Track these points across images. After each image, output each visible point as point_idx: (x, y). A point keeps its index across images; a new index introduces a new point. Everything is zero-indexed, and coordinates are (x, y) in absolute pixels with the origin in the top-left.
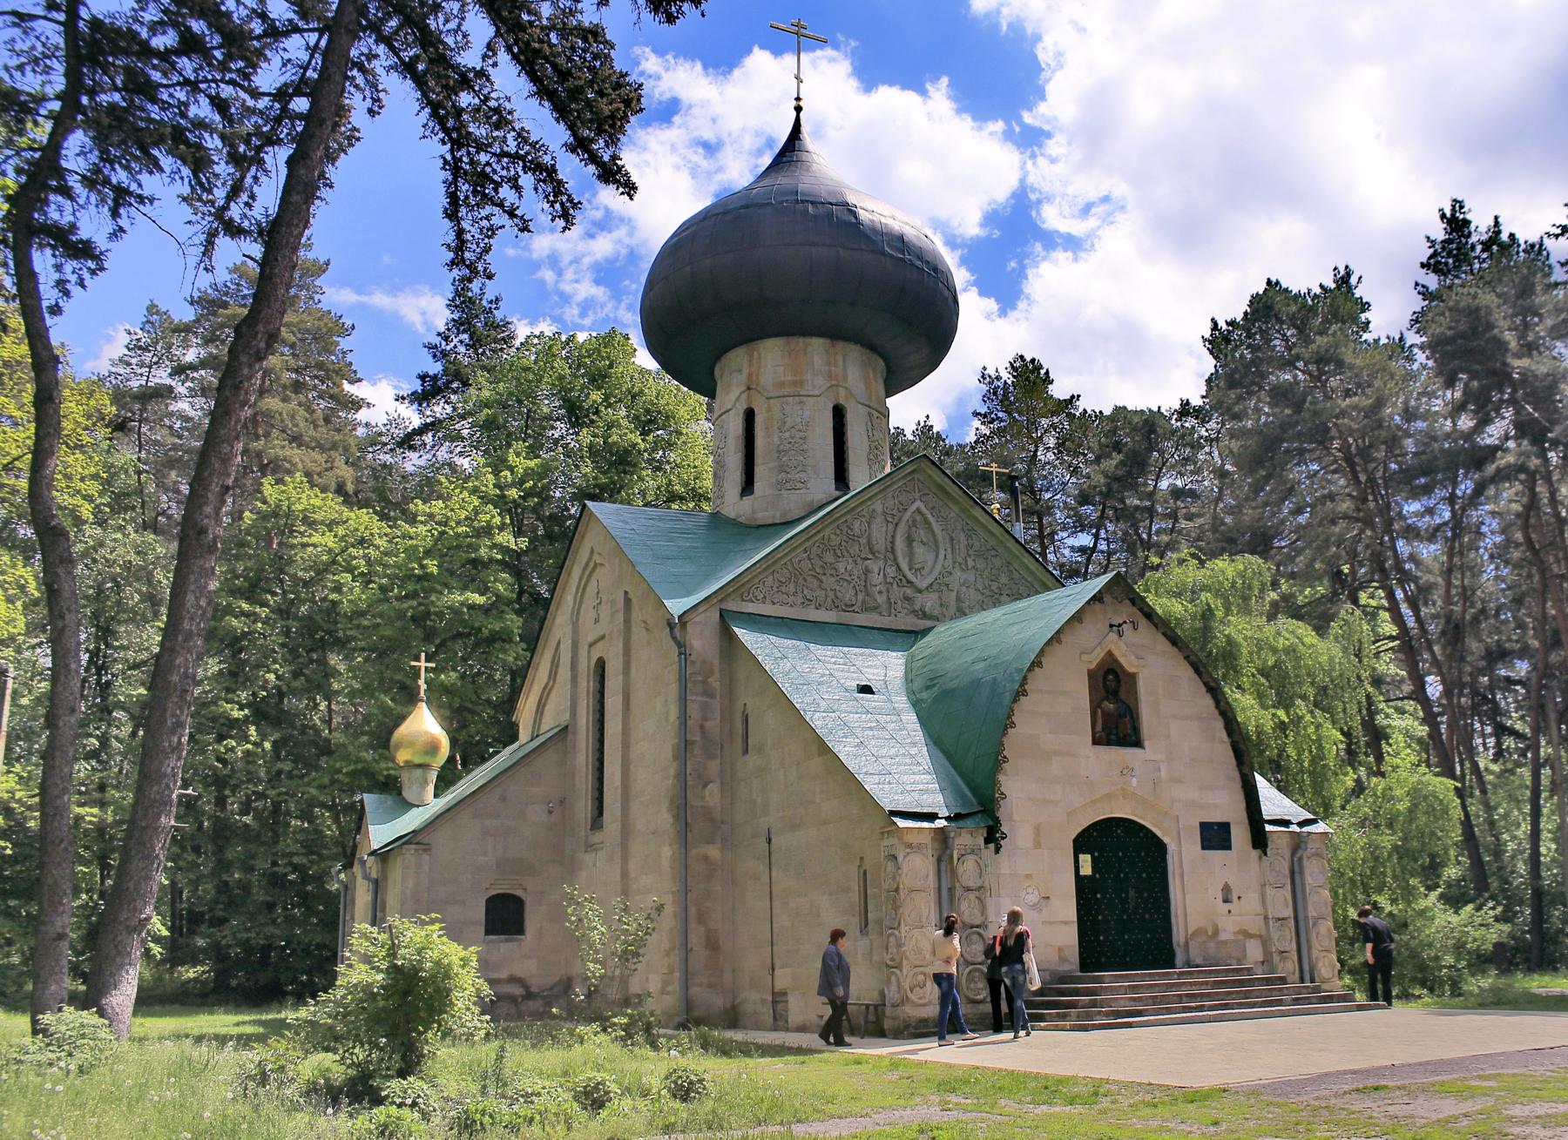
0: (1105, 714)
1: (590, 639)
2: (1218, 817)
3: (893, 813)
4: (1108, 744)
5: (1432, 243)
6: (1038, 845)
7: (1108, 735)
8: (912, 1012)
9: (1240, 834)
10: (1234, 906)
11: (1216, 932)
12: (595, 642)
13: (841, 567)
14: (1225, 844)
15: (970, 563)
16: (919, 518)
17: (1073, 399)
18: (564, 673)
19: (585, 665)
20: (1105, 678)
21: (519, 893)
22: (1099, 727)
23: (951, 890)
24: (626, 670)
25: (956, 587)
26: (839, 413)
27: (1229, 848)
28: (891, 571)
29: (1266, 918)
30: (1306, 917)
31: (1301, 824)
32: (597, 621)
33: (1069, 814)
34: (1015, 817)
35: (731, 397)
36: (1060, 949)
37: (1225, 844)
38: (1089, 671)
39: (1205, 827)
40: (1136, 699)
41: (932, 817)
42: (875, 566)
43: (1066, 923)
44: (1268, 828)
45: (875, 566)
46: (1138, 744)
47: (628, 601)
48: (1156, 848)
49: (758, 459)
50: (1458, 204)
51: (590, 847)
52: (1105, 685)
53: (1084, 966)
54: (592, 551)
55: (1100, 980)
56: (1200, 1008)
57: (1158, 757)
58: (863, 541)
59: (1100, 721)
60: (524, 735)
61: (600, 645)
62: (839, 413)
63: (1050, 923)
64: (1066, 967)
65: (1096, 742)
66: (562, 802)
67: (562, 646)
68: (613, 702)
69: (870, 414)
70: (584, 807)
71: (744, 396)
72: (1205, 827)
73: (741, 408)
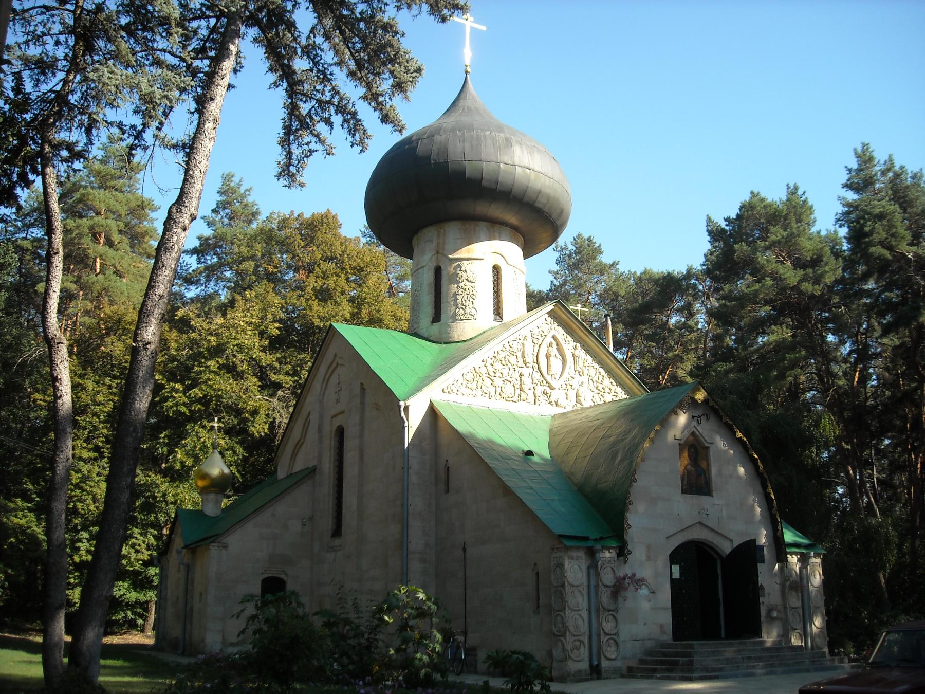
1: (333, 413)
3: (561, 536)
5: (850, 170)
8: (573, 666)
12: (336, 416)
13: (505, 372)
17: (613, 265)
18: (312, 434)
19: (329, 429)
21: (283, 576)
22: (685, 483)
23: (597, 586)
24: (361, 436)
25: (576, 386)
26: (496, 270)
28: (537, 376)
30: (809, 607)
32: (338, 401)
35: (427, 259)
36: (662, 626)
40: (708, 465)
41: (586, 539)
42: (526, 371)
43: (665, 609)
45: (526, 371)
47: (363, 389)
49: (443, 300)
50: (865, 146)
51: (332, 549)
53: (676, 636)
54: (335, 356)
55: (691, 646)
58: (519, 355)
60: (281, 474)
61: (340, 417)
62: (496, 270)
65: (684, 492)
66: (311, 519)
67: (311, 417)
68: (350, 456)
70: (327, 524)
71: (434, 258)
73: (432, 266)
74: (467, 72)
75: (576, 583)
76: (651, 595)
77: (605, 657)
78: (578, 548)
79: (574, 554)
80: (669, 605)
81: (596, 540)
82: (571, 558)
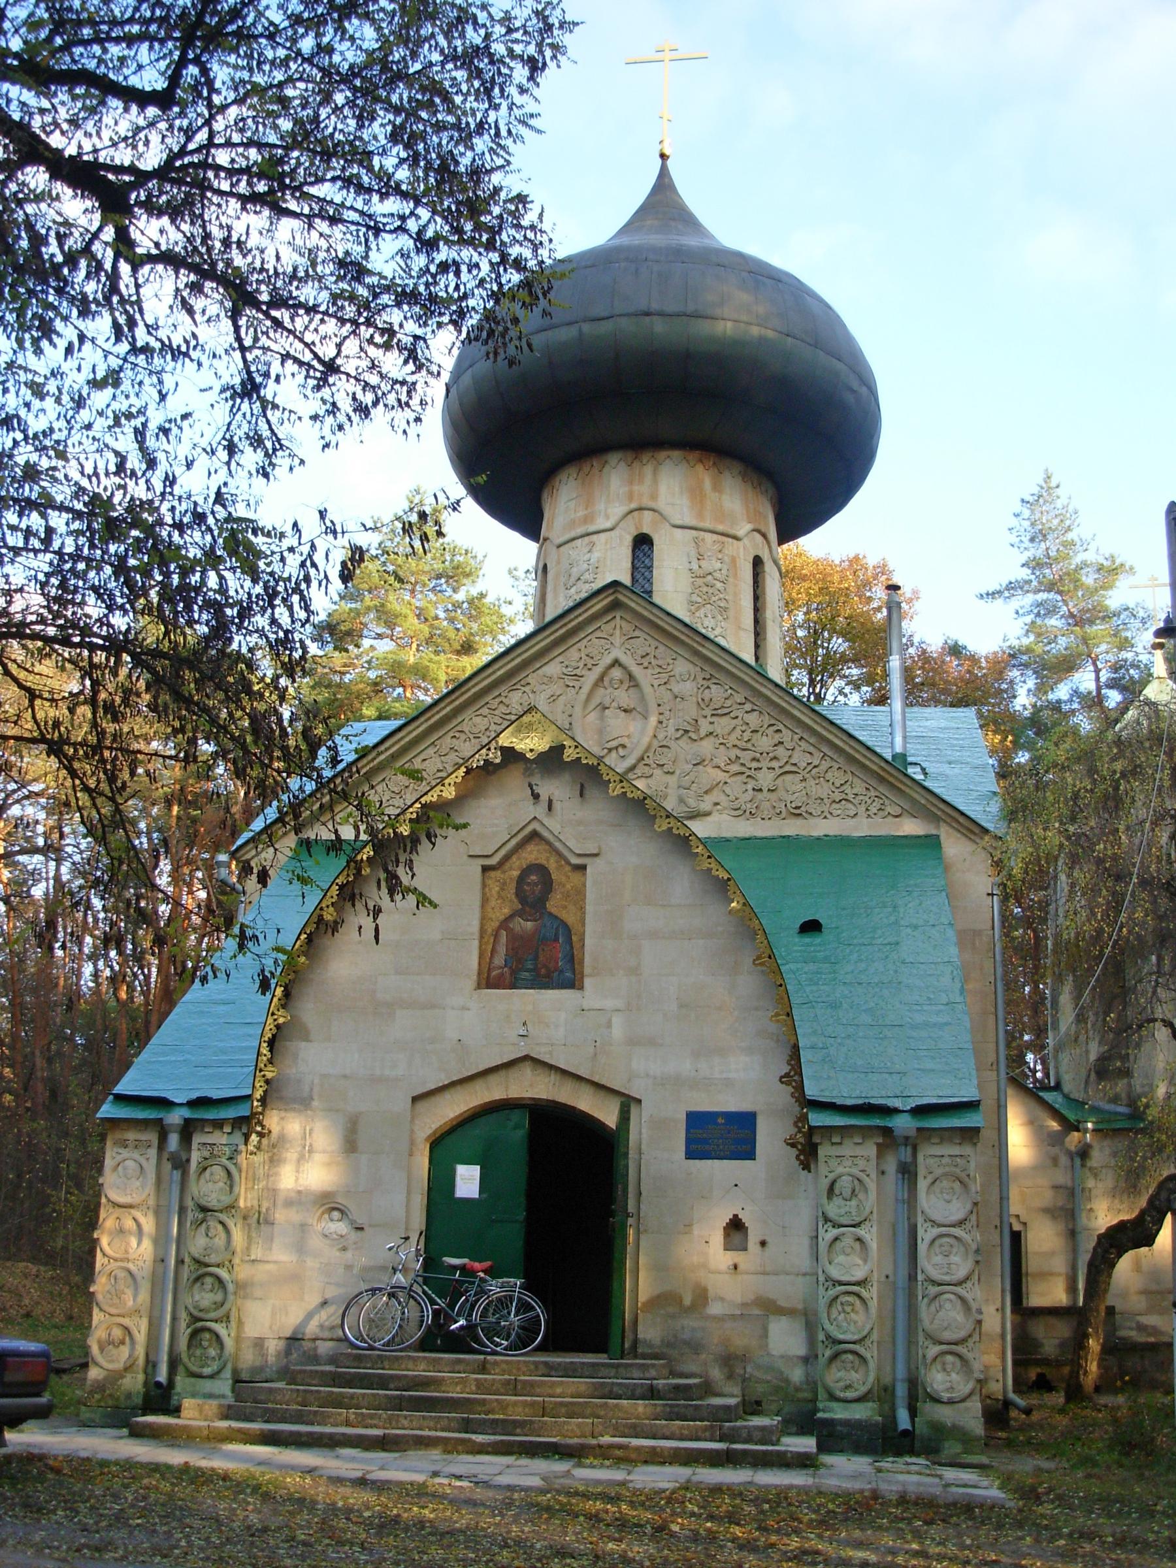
0: (513, 937)
2: (731, 1103)
7: (514, 972)
9: (771, 1137)
14: (747, 1152)
15: (705, 727)
16: (616, 673)
20: (521, 880)
22: (499, 960)
26: (643, 543)
27: (750, 1155)
31: (921, 1111)
33: (415, 1099)
37: (747, 1152)
38: (485, 869)
39: (696, 1120)
40: (582, 909)
44: (817, 1119)
46: (573, 982)
52: (519, 893)
57: (609, 1003)
59: (502, 950)
62: (643, 543)
69: (696, 541)
72: (696, 1120)
74: (663, 156)
76: (354, 1236)
77: (187, 1369)
78: (144, 1124)
79: (131, 1135)
82: (124, 1144)
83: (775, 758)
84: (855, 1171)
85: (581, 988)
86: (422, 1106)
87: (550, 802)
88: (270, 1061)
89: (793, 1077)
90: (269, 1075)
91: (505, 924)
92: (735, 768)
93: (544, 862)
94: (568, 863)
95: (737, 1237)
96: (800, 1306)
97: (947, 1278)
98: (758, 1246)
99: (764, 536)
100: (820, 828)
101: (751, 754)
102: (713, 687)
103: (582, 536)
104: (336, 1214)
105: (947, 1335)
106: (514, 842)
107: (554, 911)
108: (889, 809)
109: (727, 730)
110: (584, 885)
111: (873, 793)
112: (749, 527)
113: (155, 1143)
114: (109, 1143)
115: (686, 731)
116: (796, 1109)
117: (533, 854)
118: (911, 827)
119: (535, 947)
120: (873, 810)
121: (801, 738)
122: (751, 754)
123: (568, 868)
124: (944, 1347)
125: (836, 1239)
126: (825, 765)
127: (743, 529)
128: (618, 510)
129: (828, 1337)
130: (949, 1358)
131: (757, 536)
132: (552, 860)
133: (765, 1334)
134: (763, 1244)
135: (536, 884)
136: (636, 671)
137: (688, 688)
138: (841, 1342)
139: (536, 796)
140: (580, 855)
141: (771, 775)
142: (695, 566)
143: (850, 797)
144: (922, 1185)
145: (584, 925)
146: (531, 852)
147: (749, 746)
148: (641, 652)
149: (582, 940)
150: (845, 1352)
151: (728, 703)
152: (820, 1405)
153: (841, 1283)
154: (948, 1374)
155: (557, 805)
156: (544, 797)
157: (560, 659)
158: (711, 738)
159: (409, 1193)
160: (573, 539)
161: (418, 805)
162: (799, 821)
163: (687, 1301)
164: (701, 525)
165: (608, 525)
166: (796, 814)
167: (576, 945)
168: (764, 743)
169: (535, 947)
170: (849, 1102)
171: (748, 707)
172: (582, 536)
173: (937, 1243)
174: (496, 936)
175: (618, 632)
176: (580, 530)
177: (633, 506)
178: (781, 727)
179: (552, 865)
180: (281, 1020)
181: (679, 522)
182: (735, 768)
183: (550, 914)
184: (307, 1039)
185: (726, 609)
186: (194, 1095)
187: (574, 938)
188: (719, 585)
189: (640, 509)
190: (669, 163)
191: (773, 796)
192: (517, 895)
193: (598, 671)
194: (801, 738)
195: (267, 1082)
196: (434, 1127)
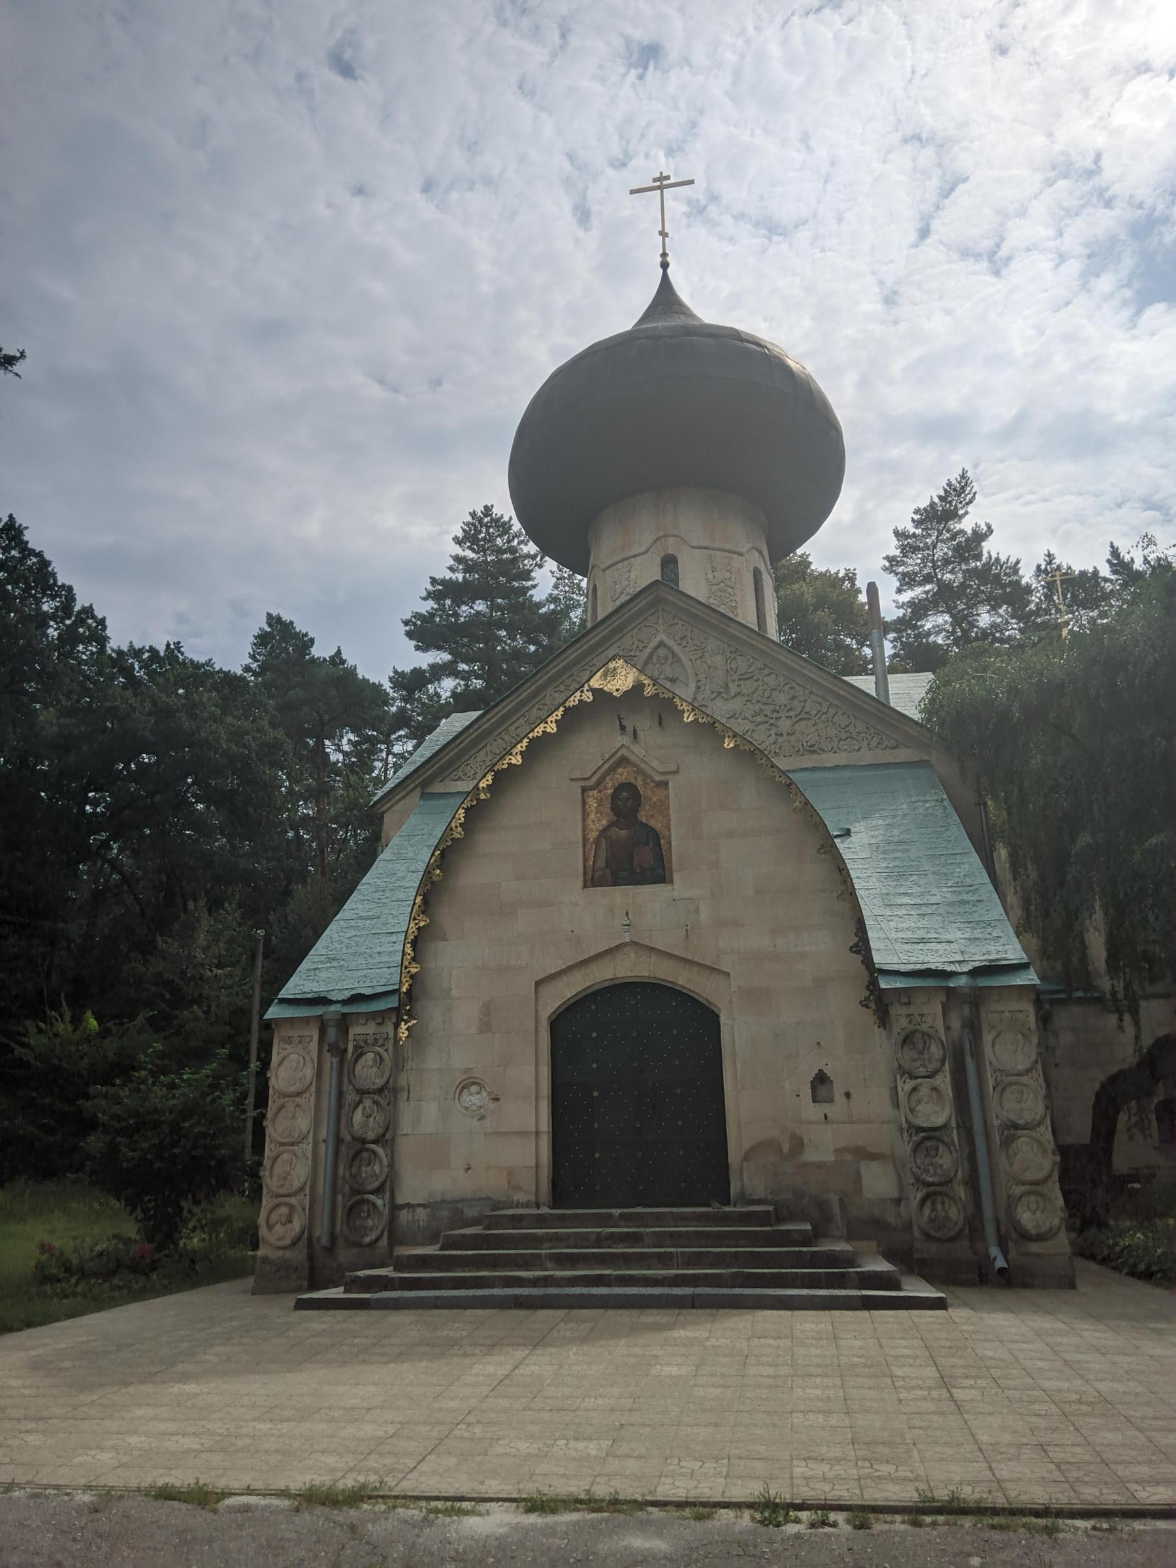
4: (615, 884)
6: (486, 1026)
10: (838, 1108)
11: (798, 1144)
15: (733, 689)
16: (662, 652)
20: (614, 796)
22: (601, 863)
29: (901, 1129)
31: (976, 972)
33: (538, 984)
34: (455, 993)
36: (510, 1173)
38: (584, 790)
40: (667, 817)
48: (704, 1021)
56: (600, 1281)
59: (603, 855)
62: (669, 563)
63: (499, 1134)
64: (520, 1197)
74: (665, 265)
75: (293, 1089)
76: (492, 1105)
79: (294, 1033)
80: (545, 1125)
81: (344, 1002)
82: (289, 1040)
83: (791, 709)
84: (924, 1027)
85: (671, 882)
86: (545, 990)
87: (635, 731)
88: (413, 959)
89: (862, 947)
90: (414, 971)
91: (603, 832)
92: (759, 719)
93: (633, 781)
94: (653, 780)
95: (822, 1090)
96: (888, 1152)
97: (1021, 1122)
98: (843, 1098)
99: (760, 552)
100: (831, 760)
101: (772, 707)
102: (739, 658)
103: (623, 560)
104: (474, 1089)
105: (1029, 1176)
106: (607, 766)
107: (644, 820)
108: (886, 743)
109: (751, 691)
110: (667, 797)
111: (872, 731)
112: (749, 545)
113: (316, 1038)
114: (275, 1041)
115: (719, 693)
116: (866, 975)
117: (622, 775)
118: (904, 755)
119: (631, 852)
120: (874, 743)
121: (811, 693)
122: (772, 707)
123: (652, 785)
124: (1027, 1187)
125: (915, 1089)
126: (832, 711)
127: (744, 547)
128: (648, 539)
129: (917, 1179)
130: (1032, 1198)
131: (756, 553)
132: (639, 779)
133: (858, 1179)
134: (848, 1095)
135: (628, 799)
136: (676, 648)
137: (719, 660)
138: (929, 1185)
139: (623, 728)
140: (661, 773)
141: (789, 722)
142: (710, 576)
143: (854, 735)
144: (988, 1038)
145: (669, 830)
146: (621, 774)
147: (770, 701)
148: (679, 636)
149: (669, 843)
150: (935, 1193)
151: (751, 669)
152: (917, 1245)
153: (923, 1130)
154: (1034, 1212)
155: (641, 734)
156: (629, 729)
157: (618, 644)
158: (739, 697)
159: (537, 1065)
160: (613, 565)
161: (526, 740)
162: (815, 756)
163: (786, 1148)
164: (712, 545)
165: (642, 549)
166: (811, 750)
167: (664, 847)
168: (782, 699)
169: (631, 852)
170: (903, 968)
171: (766, 671)
172: (623, 560)
173: (1008, 1090)
174: (597, 842)
175: (661, 621)
176: (619, 557)
177: (661, 534)
178: (794, 684)
179: (639, 783)
180: (422, 924)
181: (696, 544)
182: (759, 719)
183: (642, 823)
184: (445, 940)
185: (736, 608)
186: (347, 995)
187: (662, 842)
188: (729, 590)
189: (666, 536)
190: (669, 270)
191: (792, 738)
192: (612, 809)
193: (648, 651)
194: (811, 693)
195: (412, 977)
196: (556, 1006)
